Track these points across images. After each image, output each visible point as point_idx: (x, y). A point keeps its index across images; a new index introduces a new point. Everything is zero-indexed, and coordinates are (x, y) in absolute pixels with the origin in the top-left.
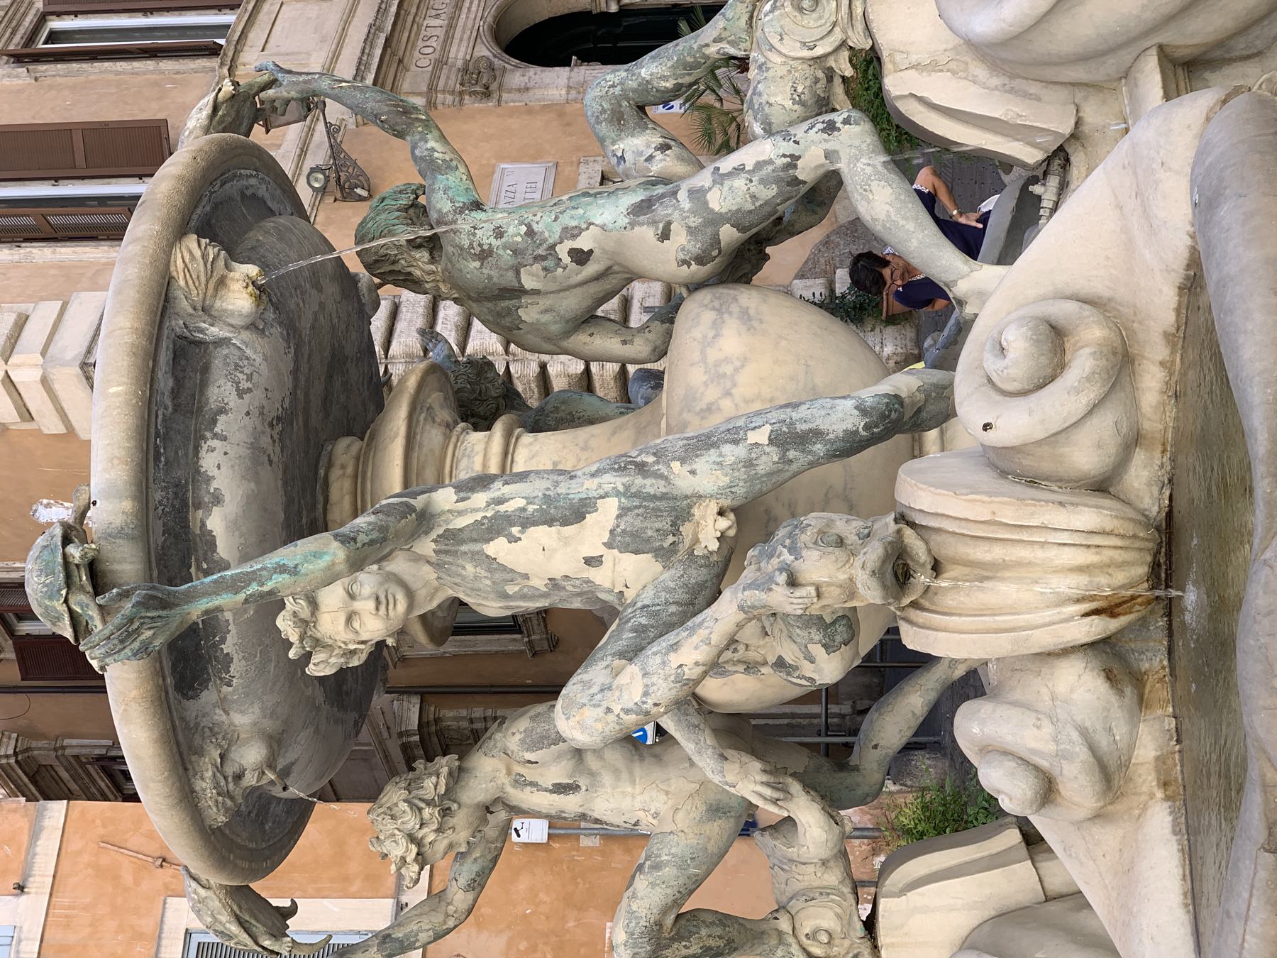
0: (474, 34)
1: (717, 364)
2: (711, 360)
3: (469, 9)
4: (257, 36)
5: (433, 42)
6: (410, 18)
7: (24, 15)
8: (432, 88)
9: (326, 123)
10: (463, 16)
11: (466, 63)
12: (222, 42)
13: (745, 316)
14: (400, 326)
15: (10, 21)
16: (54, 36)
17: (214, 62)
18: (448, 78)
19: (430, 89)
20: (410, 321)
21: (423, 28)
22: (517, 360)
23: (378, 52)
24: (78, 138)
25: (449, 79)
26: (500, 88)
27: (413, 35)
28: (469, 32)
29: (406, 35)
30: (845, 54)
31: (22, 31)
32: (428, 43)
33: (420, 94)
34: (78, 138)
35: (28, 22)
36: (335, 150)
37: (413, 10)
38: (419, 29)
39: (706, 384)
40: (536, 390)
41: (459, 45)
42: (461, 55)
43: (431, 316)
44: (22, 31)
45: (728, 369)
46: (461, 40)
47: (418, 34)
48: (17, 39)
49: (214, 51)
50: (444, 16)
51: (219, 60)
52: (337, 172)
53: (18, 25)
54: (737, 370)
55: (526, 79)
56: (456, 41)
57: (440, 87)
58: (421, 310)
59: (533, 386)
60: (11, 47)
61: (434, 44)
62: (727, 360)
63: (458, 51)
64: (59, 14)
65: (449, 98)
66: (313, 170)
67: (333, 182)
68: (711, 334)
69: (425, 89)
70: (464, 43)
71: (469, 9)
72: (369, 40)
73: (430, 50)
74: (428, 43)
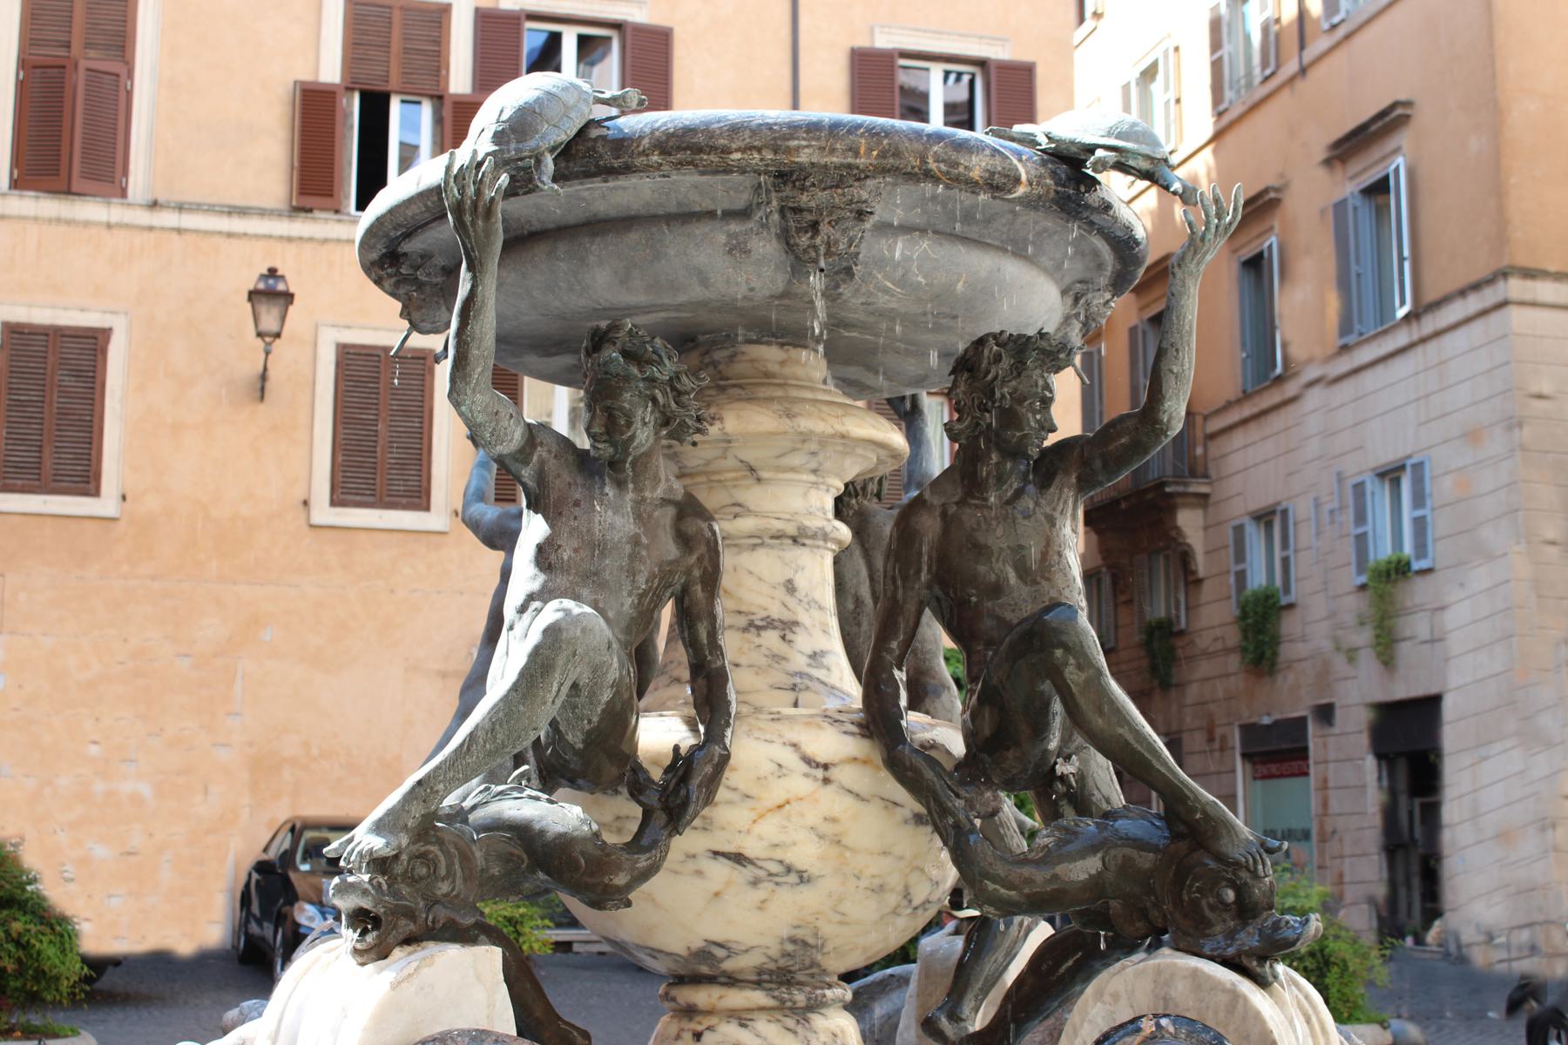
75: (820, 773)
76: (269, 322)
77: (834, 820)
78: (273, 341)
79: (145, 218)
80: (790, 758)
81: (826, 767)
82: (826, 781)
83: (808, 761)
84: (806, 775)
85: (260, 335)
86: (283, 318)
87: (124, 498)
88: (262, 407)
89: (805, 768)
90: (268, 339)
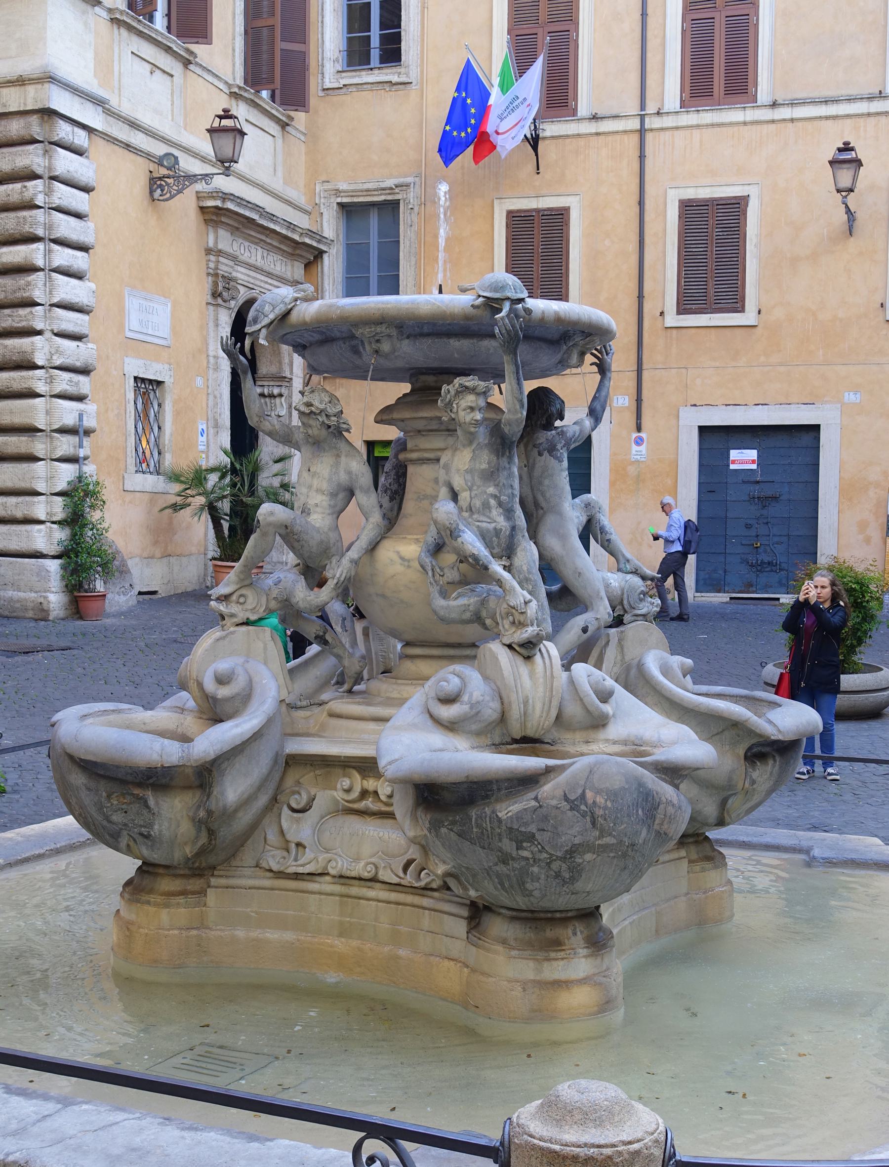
0: (251, 286)
3: (266, 282)
5: (247, 254)
6: (264, 238)
8: (220, 253)
9: (213, 174)
10: (263, 278)
11: (234, 280)
18: (227, 265)
19: (220, 251)
20: (75, 230)
21: (256, 247)
22: (45, 312)
23: (247, 213)
25: (226, 266)
26: (218, 305)
27: (253, 239)
28: (252, 282)
30: (621, 613)
32: (247, 250)
33: (216, 242)
36: (192, 178)
37: (268, 240)
38: (256, 244)
40: (19, 325)
42: (239, 275)
43: (75, 245)
46: (249, 276)
51: (242, 85)
55: (224, 325)
57: (221, 259)
59: (24, 324)
61: (246, 255)
63: (242, 273)
65: (212, 265)
69: (220, 247)
70: (246, 278)
71: (266, 282)
72: (256, 208)
74: (247, 250)
75: (406, 563)
76: (846, 181)
77: (414, 582)
78: (849, 194)
79: (767, 114)
80: (395, 557)
81: (409, 561)
82: (409, 567)
83: (402, 558)
84: (401, 564)
85: (838, 191)
86: (855, 179)
87: (759, 312)
88: (852, 239)
89: (400, 561)
90: (844, 194)
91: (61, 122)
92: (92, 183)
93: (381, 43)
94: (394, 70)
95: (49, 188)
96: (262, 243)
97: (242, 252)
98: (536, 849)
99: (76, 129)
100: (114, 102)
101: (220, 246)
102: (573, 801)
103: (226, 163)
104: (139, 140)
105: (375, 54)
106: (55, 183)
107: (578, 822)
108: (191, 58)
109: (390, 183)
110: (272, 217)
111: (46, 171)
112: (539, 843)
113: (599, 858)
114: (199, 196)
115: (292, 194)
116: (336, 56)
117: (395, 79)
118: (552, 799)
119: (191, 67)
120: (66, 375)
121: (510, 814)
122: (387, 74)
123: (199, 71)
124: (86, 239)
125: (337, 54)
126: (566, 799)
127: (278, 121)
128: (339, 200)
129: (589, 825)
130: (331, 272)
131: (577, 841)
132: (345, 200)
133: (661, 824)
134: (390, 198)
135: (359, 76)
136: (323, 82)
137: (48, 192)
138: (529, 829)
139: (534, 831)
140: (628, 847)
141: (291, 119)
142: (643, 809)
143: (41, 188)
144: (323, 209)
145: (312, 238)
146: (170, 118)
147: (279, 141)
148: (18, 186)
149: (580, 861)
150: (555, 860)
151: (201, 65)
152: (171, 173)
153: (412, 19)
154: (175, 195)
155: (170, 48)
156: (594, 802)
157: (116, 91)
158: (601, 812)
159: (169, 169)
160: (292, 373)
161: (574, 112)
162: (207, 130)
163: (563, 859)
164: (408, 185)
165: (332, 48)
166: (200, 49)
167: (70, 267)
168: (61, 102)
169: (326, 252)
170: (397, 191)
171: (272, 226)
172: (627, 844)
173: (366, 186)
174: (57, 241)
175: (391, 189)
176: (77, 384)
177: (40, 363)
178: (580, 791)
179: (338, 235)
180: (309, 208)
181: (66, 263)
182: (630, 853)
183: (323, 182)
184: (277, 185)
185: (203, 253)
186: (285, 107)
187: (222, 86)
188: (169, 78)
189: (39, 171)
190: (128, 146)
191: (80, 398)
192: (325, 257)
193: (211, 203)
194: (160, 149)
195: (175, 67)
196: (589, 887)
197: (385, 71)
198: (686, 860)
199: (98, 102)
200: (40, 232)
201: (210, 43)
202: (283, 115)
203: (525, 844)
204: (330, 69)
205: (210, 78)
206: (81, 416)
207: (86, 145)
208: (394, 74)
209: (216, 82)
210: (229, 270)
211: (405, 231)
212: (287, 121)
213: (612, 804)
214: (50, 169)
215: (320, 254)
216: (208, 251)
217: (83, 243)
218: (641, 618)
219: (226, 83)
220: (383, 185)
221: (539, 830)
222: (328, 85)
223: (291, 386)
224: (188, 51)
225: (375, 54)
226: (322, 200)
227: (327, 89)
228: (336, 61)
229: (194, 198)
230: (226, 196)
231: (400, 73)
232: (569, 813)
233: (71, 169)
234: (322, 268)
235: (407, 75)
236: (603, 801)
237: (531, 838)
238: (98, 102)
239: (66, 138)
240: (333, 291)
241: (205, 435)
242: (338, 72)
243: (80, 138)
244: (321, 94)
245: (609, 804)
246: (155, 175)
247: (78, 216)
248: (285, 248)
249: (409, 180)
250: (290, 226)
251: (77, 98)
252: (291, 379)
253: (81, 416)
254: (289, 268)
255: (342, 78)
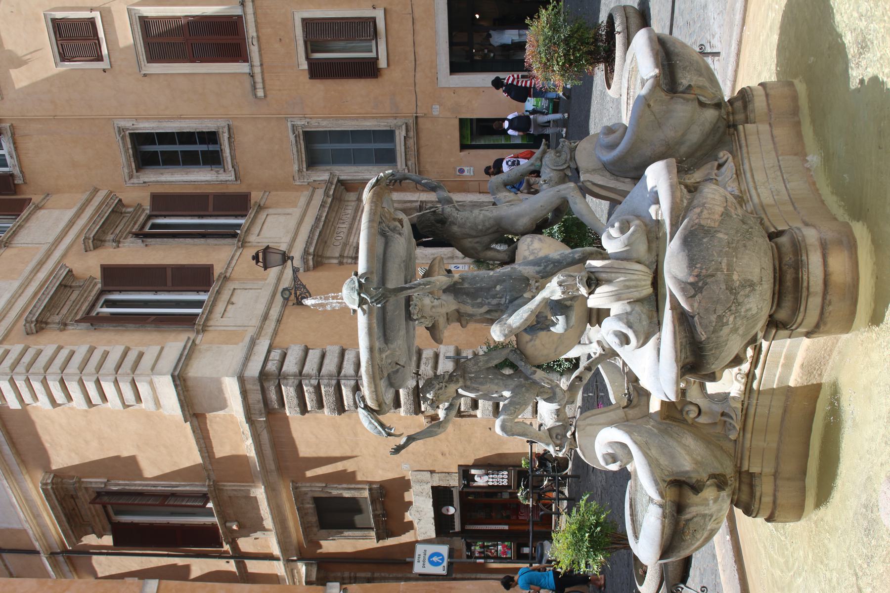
1: (533, 250)
2: (530, 250)
4: (256, 229)
6: (331, 223)
7: (140, 216)
8: (342, 256)
9: (293, 267)
12: (238, 232)
13: (540, 240)
14: (326, 361)
15: (133, 218)
16: (154, 226)
17: (235, 241)
18: (349, 250)
24: (169, 273)
27: (332, 231)
29: (328, 231)
31: (139, 223)
32: (339, 235)
34: (169, 273)
35: (142, 218)
36: (295, 278)
37: (332, 220)
38: (335, 228)
39: (529, 255)
41: (355, 236)
44: (139, 223)
45: (536, 251)
46: (355, 234)
47: (334, 231)
48: (136, 227)
49: (235, 236)
50: (346, 223)
51: (237, 239)
52: (295, 291)
53: (137, 220)
54: (538, 252)
56: (353, 234)
58: (336, 355)
60: (134, 230)
61: (342, 236)
62: (535, 249)
63: (354, 239)
64: (157, 216)
65: (350, 261)
66: (284, 290)
67: (293, 296)
68: (530, 243)
72: (312, 232)
73: (340, 238)
74: (339, 235)
91: (266, 368)
92: (302, 347)
93: (205, 143)
94: (221, 136)
95: (307, 376)
96: (334, 224)
97: (340, 238)
98: (728, 313)
99: (270, 358)
100: (251, 332)
101: (337, 255)
102: (695, 291)
103: (285, 258)
104: (274, 313)
105: (212, 147)
106: (303, 372)
107: (710, 287)
108: (223, 276)
109: (292, 137)
110: (318, 219)
111: (297, 378)
112: (724, 312)
113: (737, 269)
114: (307, 270)
115: (303, 201)
116: (215, 173)
117: (226, 135)
118: (693, 306)
119: (228, 275)
120: (422, 367)
121: (703, 333)
122: (224, 140)
123: (230, 270)
124: (337, 352)
125: (213, 172)
126: (694, 296)
127: (257, 213)
128: (305, 170)
129: (713, 279)
130: (351, 174)
131: (723, 287)
132: (305, 166)
133: (715, 221)
134: (302, 137)
135: (226, 158)
136: (232, 181)
137: (309, 377)
138: (714, 320)
139: (715, 316)
140: (729, 248)
141: (256, 202)
142: (703, 238)
143: (307, 381)
144: (311, 180)
145: (330, 189)
146: (259, 291)
147: (270, 211)
148: (306, 394)
149: (738, 282)
150: (737, 299)
151: (227, 269)
152: (293, 292)
153: (189, 125)
154: (307, 289)
155: (217, 291)
156: (697, 276)
157: (246, 328)
158: (704, 271)
159: (291, 294)
160: (417, 201)
161: (240, 17)
162: (265, 270)
163: (736, 294)
164: (293, 126)
165: (210, 175)
166: (217, 271)
167: (354, 363)
168: (254, 370)
169: (338, 178)
170: (297, 133)
171: (323, 218)
172: (727, 249)
173: (295, 153)
174: (339, 372)
175: (296, 137)
176: (427, 359)
177: (415, 384)
178: (689, 287)
179: (327, 170)
180: (311, 189)
181: (352, 366)
182: (734, 245)
183: (294, 180)
184: (297, 212)
185: (342, 266)
186: (249, 208)
187: (238, 254)
188: (236, 291)
189: (296, 382)
190: (279, 321)
191: (437, 356)
192: (342, 178)
193: (311, 263)
194: (279, 300)
195: (230, 286)
196: (757, 270)
197: (222, 141)
198: (746, 125)
199: (253, 343)
200: (334, 382)
201: (212, 265)
202: (253, 209)
203: (725, 321)
204: (223, 177)
205: (234, 262)
206: (447, 358)
207: (279, 351)
208: (223, 136)
209: (236, 257)
210: (352, 247)
211: (323, 127)
212: (257, 206)
213: (699, 263)
214: (295, 375)
215: (341, 182)
216: (341, 263)
217: (339, 353)
218: (573, 154)
219: (236, 251)
220: (294, 142)
221: (715, 313)
222: (233, 178)
223: (425, 201)
224: (218, 279)
225: (212, 147)
226: (305, 180)
227: (236, 178)
228: (217, 172)
229: (309, 273)
230: (306, 252)
231: (223, 132)
232: (704, 293)
233: (295, 361)
234: (349, 180)
235: (223, 127)
236: (696, 270)
237: (720, 318)
238: (253, 343)
239: (276, 365)
240: (363, 173)
241: (459, 265)
242: (224, 171)
243: (276, 355)
244: (239, 182)
245: (698, 266)
246: (295, 302)
247: (323, 356)
248: (336, 209)
249: (289, 124)
250: (322, 205)
251: (252, 358)
252: (421, 201)
253: (447, 358)
254: (349, 203)
255: (228, 169)
